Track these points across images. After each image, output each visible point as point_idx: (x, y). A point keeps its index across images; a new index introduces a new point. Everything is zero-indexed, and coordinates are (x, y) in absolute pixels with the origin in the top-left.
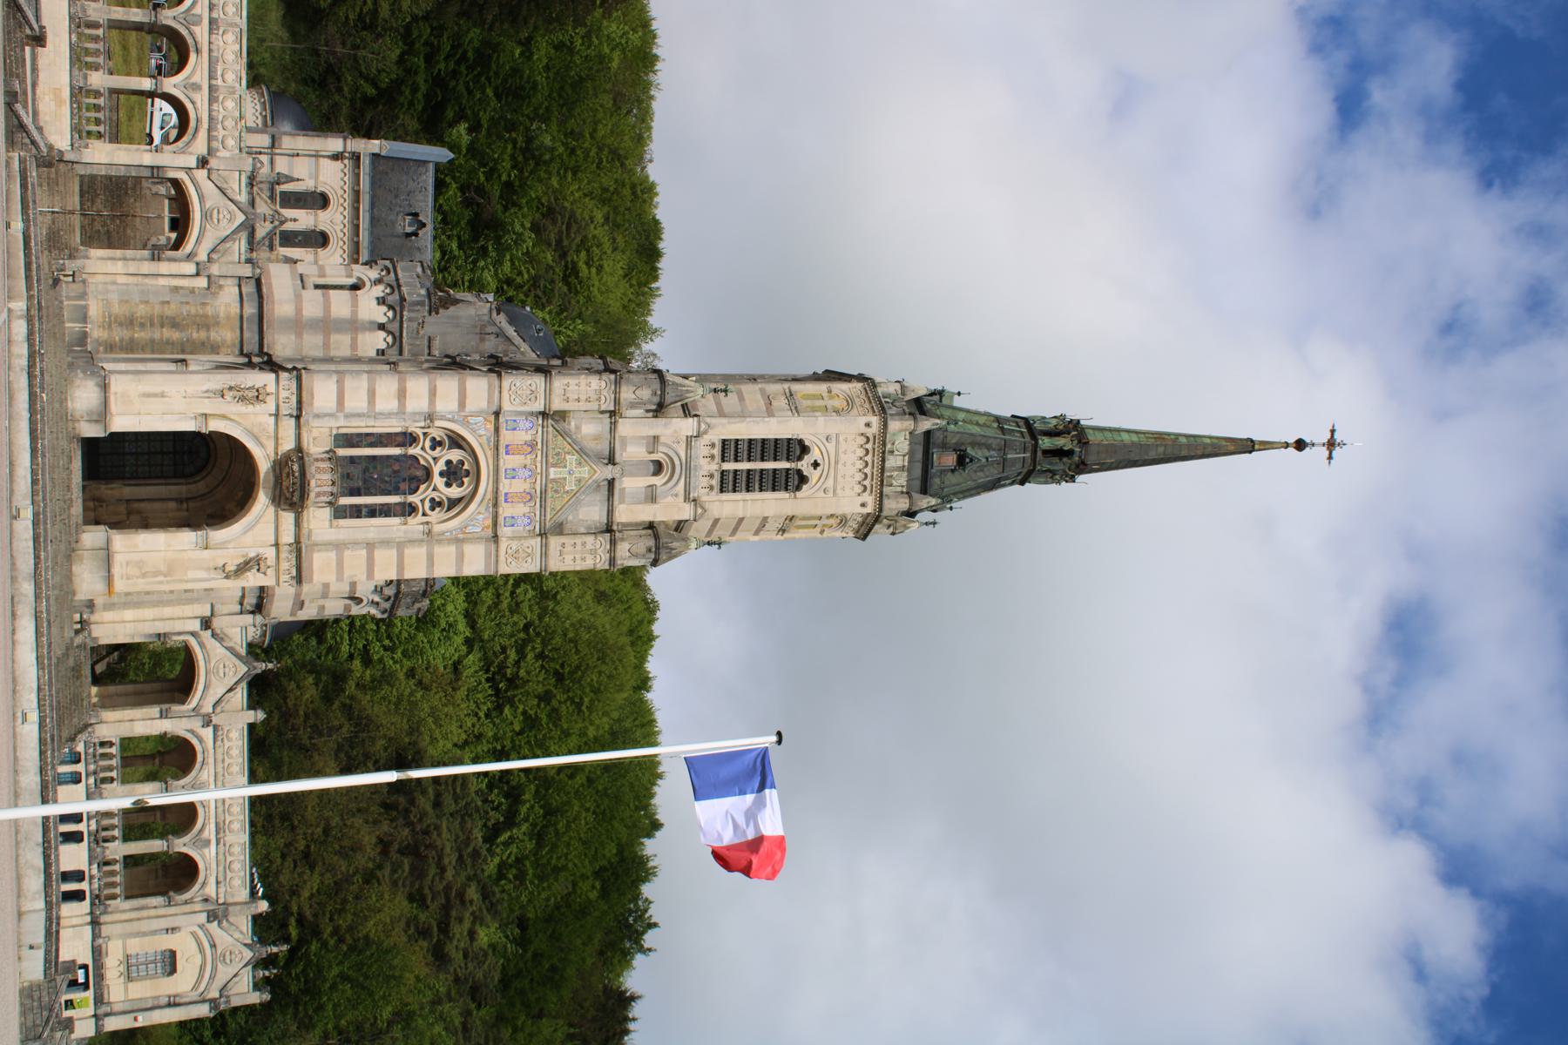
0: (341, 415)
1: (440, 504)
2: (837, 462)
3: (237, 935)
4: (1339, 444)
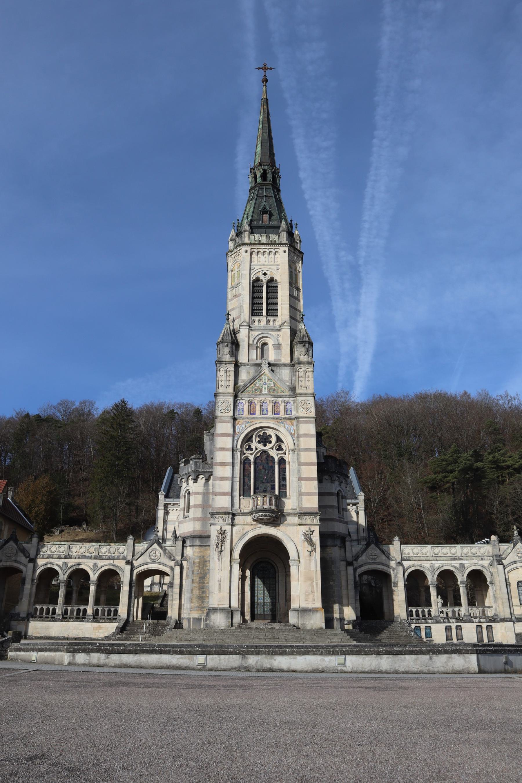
1: (280, 446)
3: (509, 551)
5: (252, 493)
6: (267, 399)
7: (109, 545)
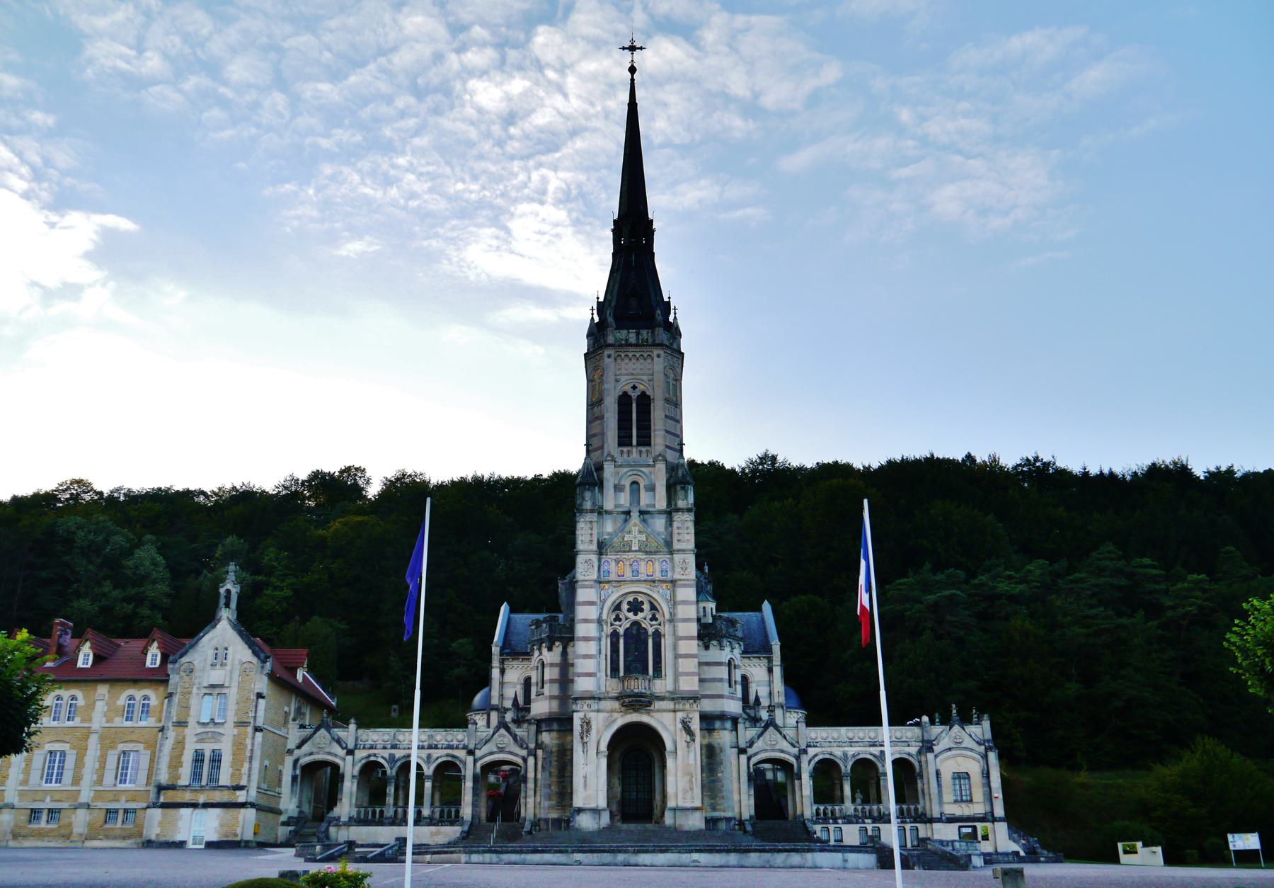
0: (598, 675)
2: (633, 374)
3: (944, 735)
4: (632, 43)
5: (622, 674)
6: (637, 557)
7: (446, 731)
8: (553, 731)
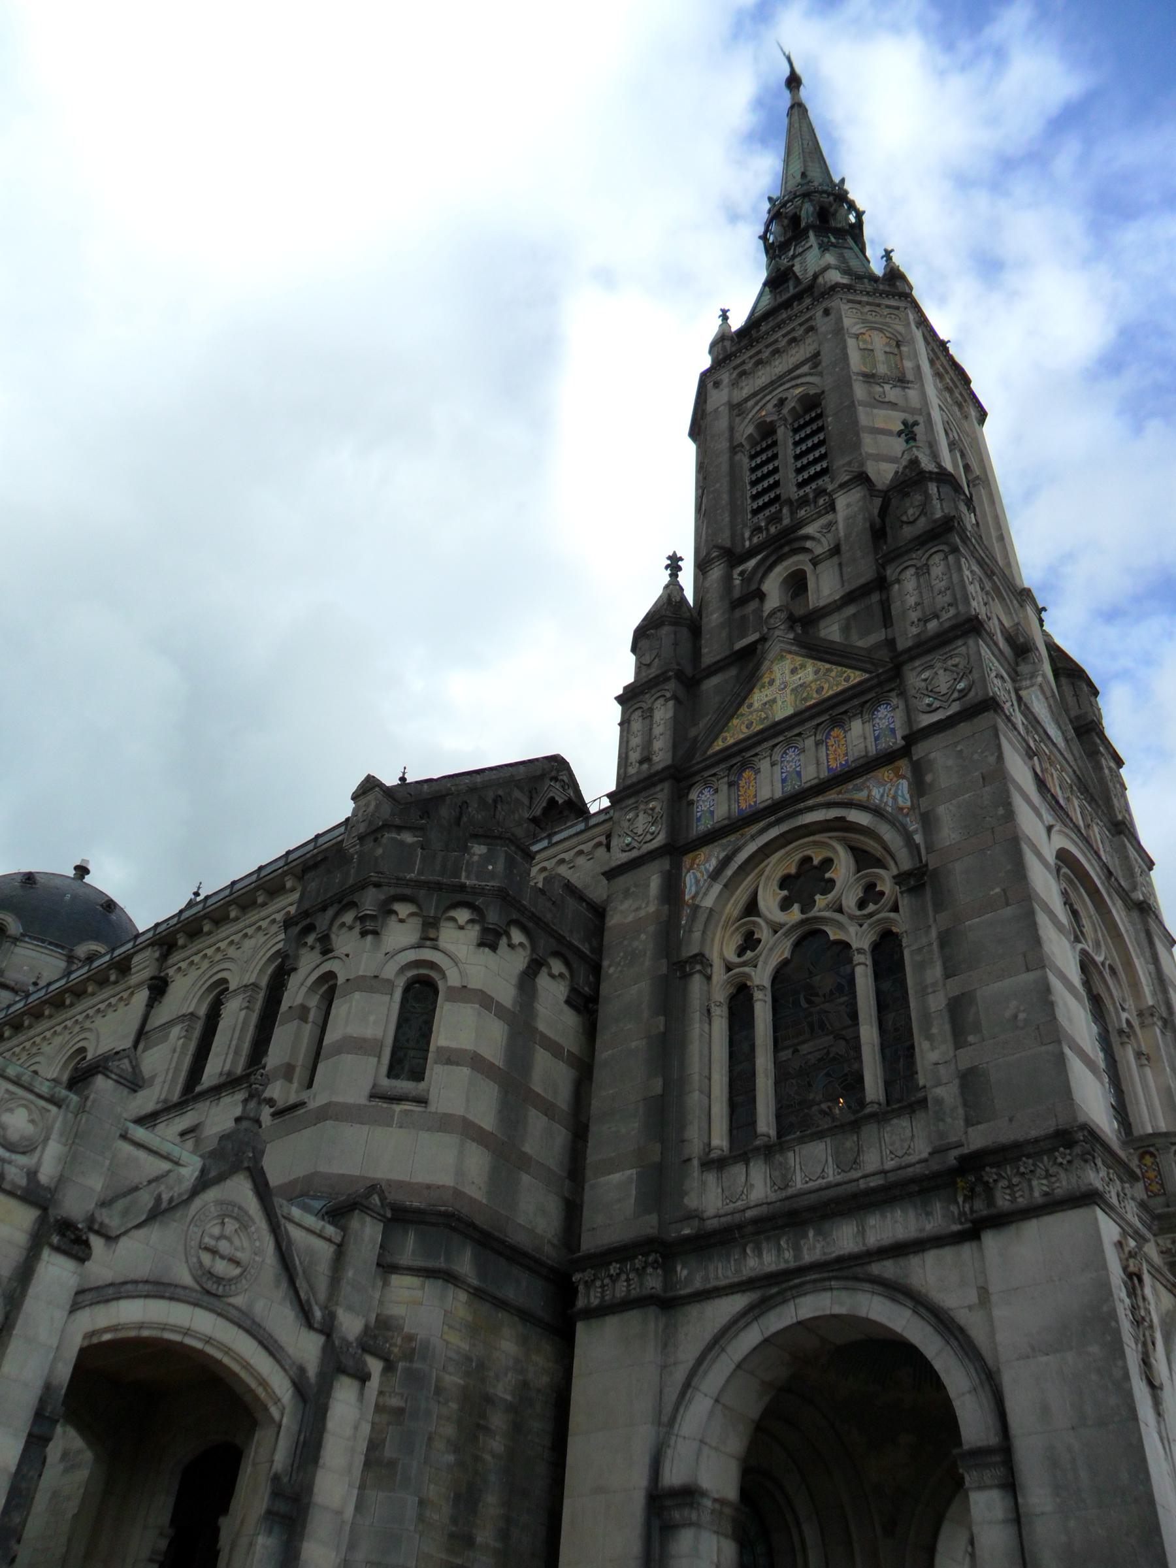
8: (449, 1277)
